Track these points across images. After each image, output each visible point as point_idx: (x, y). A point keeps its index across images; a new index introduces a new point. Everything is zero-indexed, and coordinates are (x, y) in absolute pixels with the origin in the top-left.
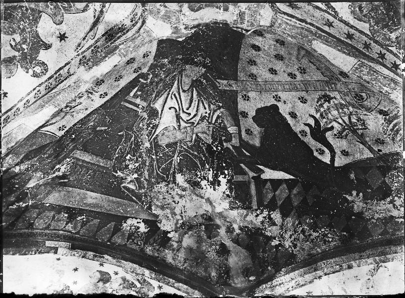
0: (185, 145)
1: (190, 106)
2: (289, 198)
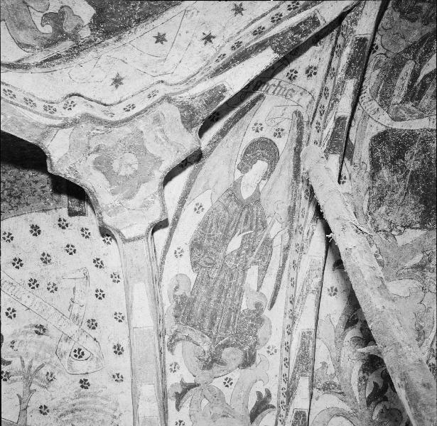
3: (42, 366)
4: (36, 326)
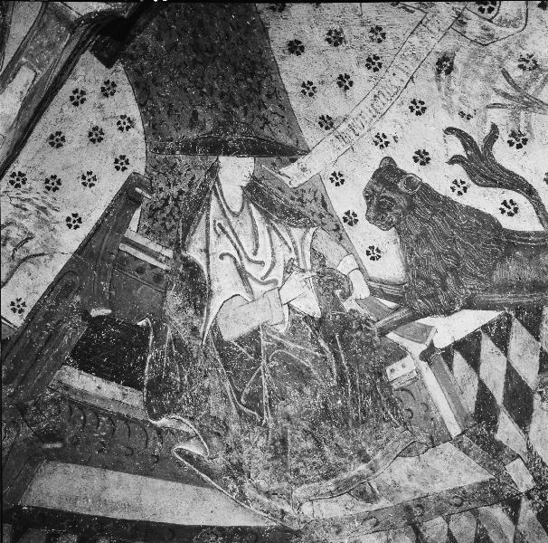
0: (274, 333)
1: (257, 245)
2: (511, 372)
3: (506, 74)
4: (439, 72)
